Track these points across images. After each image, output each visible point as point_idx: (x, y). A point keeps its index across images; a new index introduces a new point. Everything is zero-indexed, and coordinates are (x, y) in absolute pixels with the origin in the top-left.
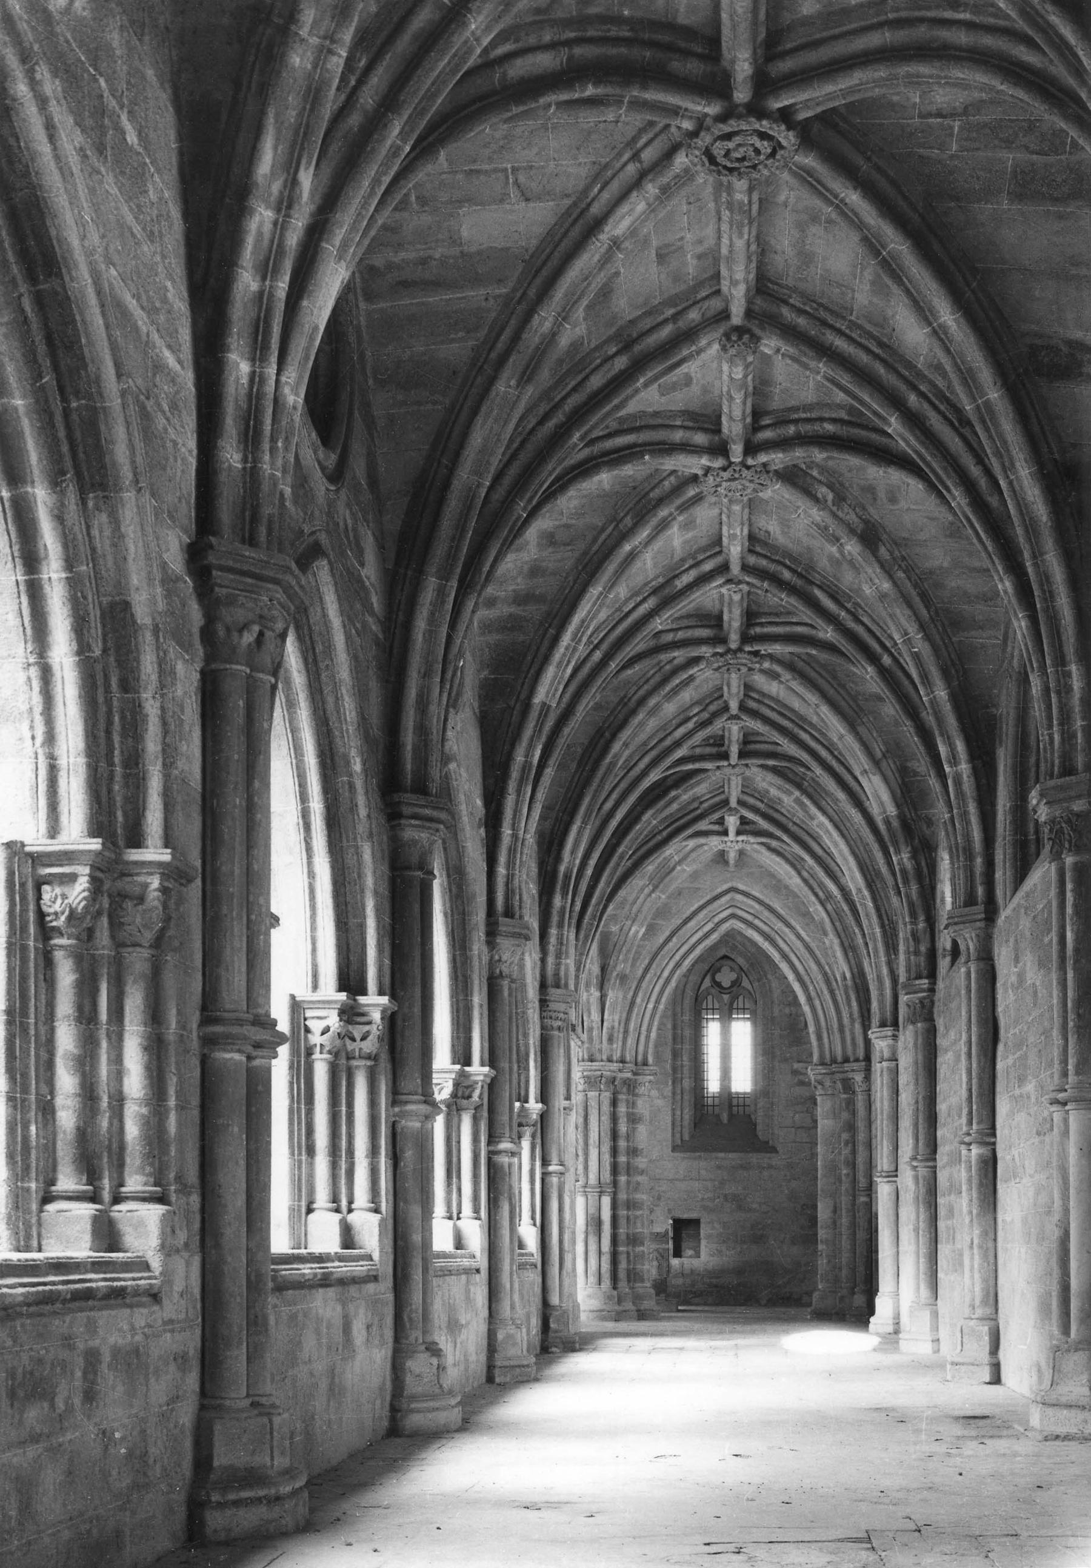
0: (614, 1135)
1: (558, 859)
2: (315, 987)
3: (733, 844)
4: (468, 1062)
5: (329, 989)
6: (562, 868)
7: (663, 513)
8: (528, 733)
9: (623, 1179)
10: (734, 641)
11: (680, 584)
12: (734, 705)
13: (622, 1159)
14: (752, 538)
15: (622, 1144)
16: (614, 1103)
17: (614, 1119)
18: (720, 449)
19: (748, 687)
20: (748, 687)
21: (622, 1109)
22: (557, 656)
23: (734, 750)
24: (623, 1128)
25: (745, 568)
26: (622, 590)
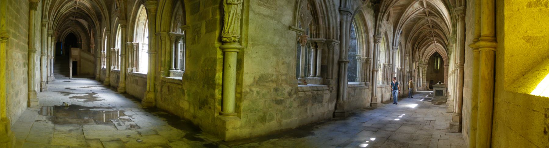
0: (423, 72)
1: (414, 47)
2: (385, 63)
3: (436, 44)
4: (402, 67)
5: (386, 63)
6: (415, 47)
7: (421, 19)
8: (409, 38)
9: (423, 76)
10: (431, 28)
11: (425, 24)
12: (433, 33)
13: (423, 74)
14: (431, 20)
15: (424, 73)
16: (423, 69)
17: (423, 70)
18: (426, 15)
19: (434, 31)
20: (434, 31)
21: (424, 69)
22: (412, 31)
23: (434, 36)
24: (424, 71)
25: (431, 23)
26: (419, 25)
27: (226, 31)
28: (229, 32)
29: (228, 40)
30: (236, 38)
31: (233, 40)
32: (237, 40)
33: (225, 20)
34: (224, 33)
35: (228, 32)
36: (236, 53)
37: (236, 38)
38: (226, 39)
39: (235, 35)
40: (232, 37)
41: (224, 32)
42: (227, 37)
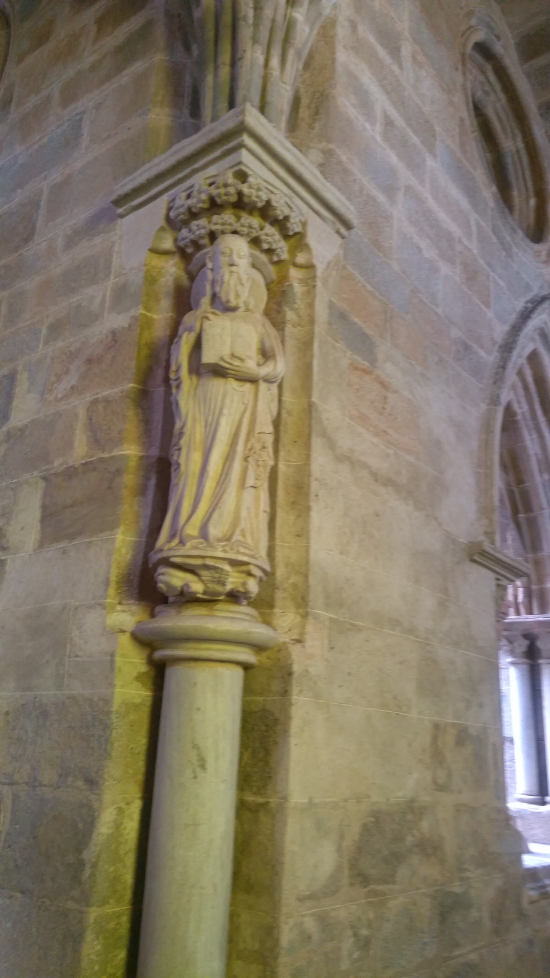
27: (192, 530)
28: (214, 531)
29: (197, 587)
30: (249, 574)
31: (229, 587)
32: (253, 586)
33: (182, 460)
34: (176, 541)
35: (204, 534)
36: (239, 672)
37: (249, 574)
38: (189, 577)
39: (246, 559)
40: (227, 567)
41: (172, 536)
42: (199, 562)
